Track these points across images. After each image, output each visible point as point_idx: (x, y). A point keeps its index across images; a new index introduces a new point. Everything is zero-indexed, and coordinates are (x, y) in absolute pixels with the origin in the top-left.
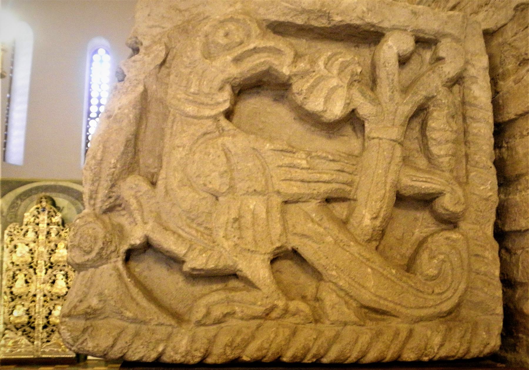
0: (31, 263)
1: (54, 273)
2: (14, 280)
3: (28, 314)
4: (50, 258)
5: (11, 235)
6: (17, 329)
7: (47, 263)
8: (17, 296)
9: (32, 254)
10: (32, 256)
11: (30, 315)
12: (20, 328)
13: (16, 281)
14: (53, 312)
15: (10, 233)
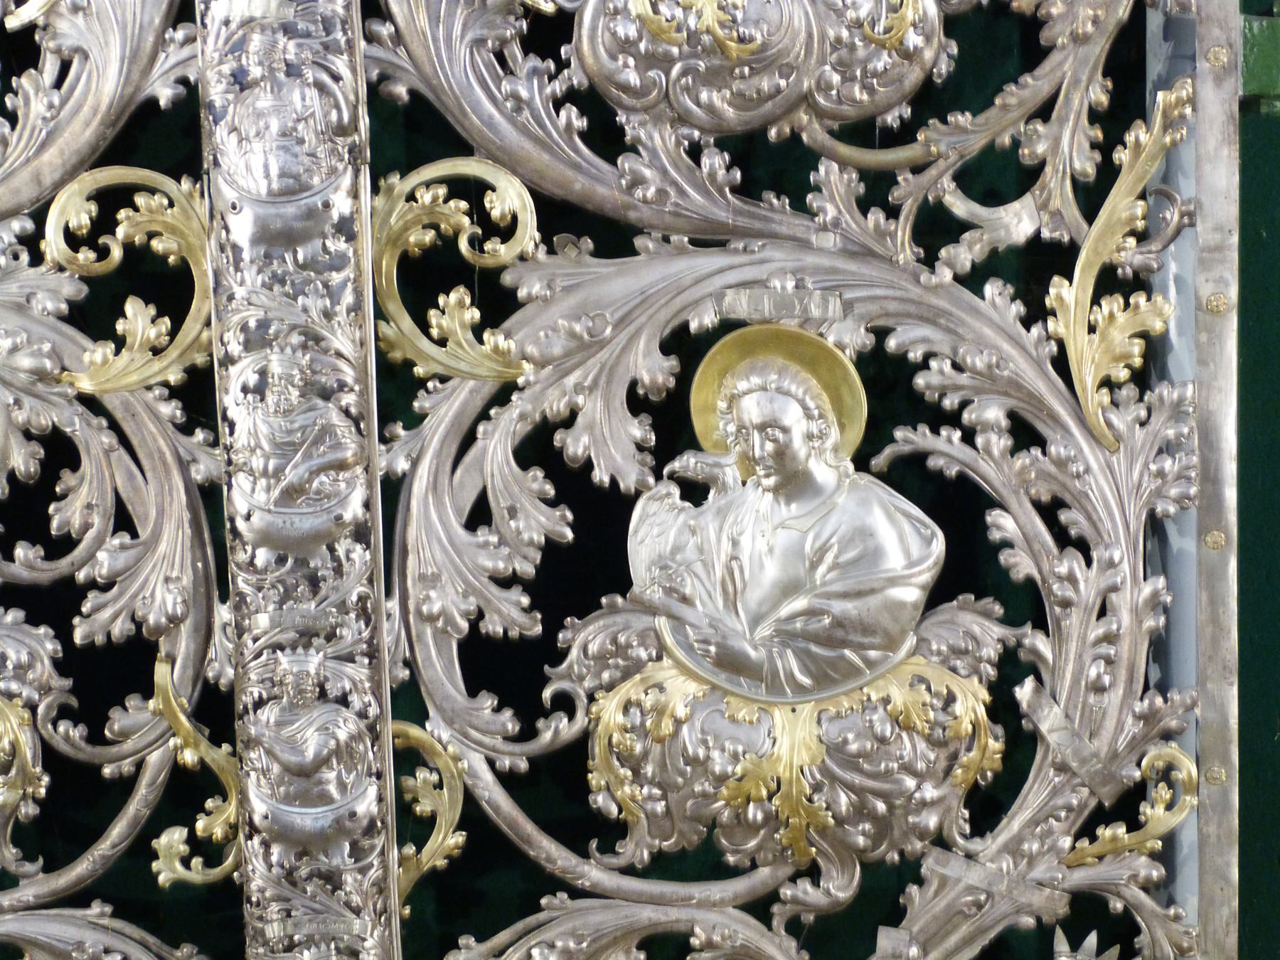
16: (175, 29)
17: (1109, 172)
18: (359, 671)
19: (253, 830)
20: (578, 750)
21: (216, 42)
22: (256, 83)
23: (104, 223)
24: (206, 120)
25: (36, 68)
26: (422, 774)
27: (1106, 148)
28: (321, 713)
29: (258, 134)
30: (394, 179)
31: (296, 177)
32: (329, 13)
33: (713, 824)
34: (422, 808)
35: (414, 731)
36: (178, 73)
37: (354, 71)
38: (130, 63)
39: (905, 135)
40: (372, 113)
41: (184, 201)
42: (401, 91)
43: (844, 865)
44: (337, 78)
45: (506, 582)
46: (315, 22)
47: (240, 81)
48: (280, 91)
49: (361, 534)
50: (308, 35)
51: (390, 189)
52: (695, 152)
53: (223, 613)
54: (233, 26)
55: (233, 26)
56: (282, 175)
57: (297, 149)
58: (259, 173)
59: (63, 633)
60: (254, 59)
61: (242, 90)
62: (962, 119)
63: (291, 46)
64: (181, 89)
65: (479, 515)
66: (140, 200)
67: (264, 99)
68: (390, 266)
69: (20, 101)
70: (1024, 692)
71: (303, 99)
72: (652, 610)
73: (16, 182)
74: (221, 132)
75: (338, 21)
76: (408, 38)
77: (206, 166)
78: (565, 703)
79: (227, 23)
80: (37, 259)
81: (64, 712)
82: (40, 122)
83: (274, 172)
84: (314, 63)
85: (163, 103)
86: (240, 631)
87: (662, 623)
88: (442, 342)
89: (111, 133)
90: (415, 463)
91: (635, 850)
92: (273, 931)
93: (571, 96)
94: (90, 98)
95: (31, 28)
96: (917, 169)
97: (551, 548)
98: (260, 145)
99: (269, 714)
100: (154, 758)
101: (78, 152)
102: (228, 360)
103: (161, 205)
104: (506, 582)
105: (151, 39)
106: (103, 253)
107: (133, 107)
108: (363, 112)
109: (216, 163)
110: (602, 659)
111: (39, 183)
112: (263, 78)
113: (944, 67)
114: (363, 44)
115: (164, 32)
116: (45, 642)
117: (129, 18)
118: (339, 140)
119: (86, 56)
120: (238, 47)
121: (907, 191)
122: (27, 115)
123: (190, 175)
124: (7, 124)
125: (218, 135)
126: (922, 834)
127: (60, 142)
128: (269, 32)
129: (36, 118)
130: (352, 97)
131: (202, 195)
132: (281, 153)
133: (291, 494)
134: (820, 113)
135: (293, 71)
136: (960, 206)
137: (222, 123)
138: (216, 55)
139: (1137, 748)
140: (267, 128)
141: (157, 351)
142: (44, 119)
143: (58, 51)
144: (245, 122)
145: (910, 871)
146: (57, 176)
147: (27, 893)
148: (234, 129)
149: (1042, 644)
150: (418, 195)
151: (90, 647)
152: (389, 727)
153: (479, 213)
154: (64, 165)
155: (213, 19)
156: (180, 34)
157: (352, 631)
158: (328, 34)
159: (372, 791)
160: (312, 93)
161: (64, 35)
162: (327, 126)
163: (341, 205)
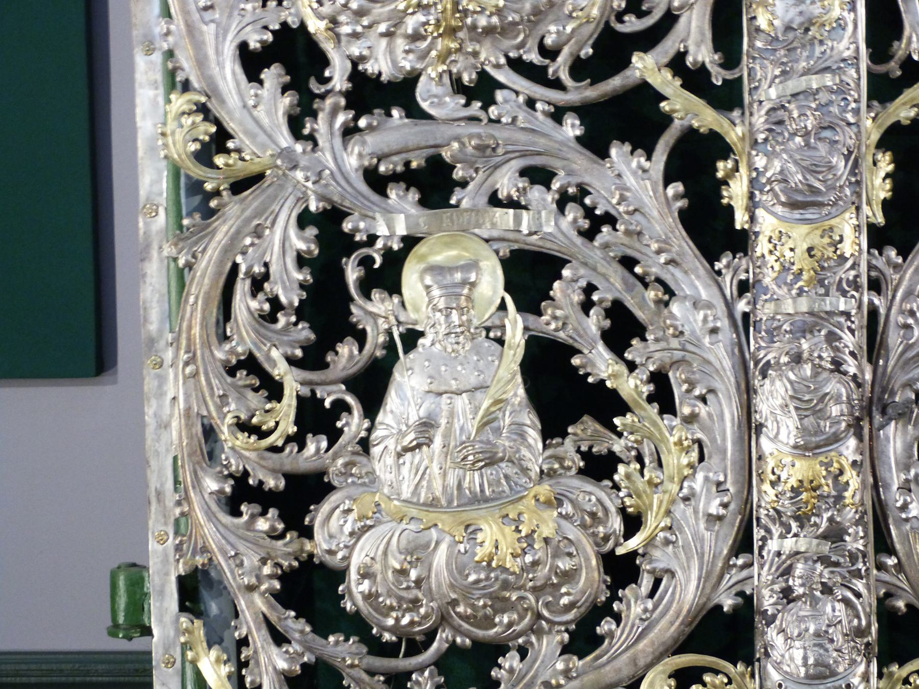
16: (737, 558)
21: (770, 569)
22: (799, 598)
24: (758, 621)
25: (636, 584)
29: (799, 635)
30: (895, 668)
31: (827, 666)
32: (854, 551)
36: (738, 588)
37: (869, 590)
38: (705, 582)
40: (878, 622)
41: (739, 678)
42: (901, 604)
44: (858, 595)
46: (843, 556)
47: (787, 595)
48: (817, 604)
50: (837, 564)
51: (891, 674)
54: (784, 557)
55: (784, 557)
56: (817, 664)
57: (828, 646)
58: (799, 661)
60: (798, 582)
61: (788, 603)
63: (826, 573)
64: (740, 600)
66: (707, 678)
67: (803, 609)
69: (623, 607)
71: (834, 610)
73: (618, 663)
74: (772, 635)
75: (860, 555)
76: (907, 568)
77: (758, 656)
79: (779, 554)
82: (637, 621)
83: (811, 661)
84: (842, 585)
85: (725, 609)
89: (688, 630)
94: (674, 605)
95: (634, 554)
98: (802, 643)
101: (663, 643)
103: (722, 682)
105: (720, 565)
107: (704, 612)
108: (874, 618)
109: (767, 655)
111: (636, 665)
112: (804, 594)
114: (875, 572)
115: (729, 560)
117: (707, 549)
118: (858, 640)
119: (672, 574)
120: (788, 572)
122: (628, 616)
123: (743, 661)
124: (614, 622)
125: (769, 635)
127: (652, 635)
128: (810, 563)
129: (635, 619)
130: (868, 610)
131: (753, 676)
132: (816, 649)
135: (827, 590)
137: (772, 626)
138: (770, 578)
140: (807, 630)
142: (641, 619)
143: (652, 572)
144: (791, 626)
146: (649, 659)
148: (782, 631)
150: (912, 680)
154: (653, 653)
155: (769, 551)
156: (740, 562)
158: (853, 565)
160: (840, 606)
161: (657, 560)
162: (850, 630)
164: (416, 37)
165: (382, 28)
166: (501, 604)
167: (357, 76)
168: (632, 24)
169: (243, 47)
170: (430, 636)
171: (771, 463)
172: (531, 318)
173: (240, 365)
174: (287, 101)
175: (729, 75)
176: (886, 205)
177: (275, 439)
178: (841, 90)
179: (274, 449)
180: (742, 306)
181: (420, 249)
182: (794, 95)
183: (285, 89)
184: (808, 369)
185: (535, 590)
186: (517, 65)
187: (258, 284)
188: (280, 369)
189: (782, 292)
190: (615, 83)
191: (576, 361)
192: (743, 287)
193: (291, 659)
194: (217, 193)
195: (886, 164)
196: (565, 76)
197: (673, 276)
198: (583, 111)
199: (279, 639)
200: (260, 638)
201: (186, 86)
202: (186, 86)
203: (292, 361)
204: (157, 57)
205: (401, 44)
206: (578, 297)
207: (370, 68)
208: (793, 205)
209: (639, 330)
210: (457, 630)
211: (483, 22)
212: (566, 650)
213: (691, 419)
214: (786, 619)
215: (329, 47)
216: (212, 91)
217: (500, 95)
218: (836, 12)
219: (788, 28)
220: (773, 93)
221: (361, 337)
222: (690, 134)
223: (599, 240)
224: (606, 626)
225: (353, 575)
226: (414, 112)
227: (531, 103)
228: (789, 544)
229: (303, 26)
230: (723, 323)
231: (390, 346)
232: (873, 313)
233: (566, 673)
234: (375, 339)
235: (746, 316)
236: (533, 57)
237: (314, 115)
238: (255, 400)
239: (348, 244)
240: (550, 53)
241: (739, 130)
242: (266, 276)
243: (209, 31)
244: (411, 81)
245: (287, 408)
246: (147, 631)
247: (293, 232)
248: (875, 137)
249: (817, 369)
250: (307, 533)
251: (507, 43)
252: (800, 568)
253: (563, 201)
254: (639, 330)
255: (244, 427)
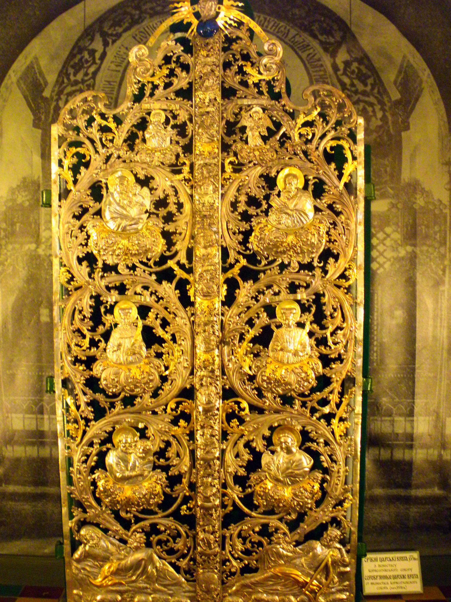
0: (163, 259)
1: (267, 299)
2: (101, 329)
3: (166, 469)
4: (247, 234)
5: (79, 144)
6: (126, 524)
7: (232, 255)
8: (115, 396)
9: (169, 218)
10: (170, 228)
11: (173, 472)
12: (138, 520)
13: (107, 336)
14: (266, 459)
15: (72, 136)
17: (341, 402)
18: (216, 481)
19: (198, 506)
20: (252, 494)
23: (177, 407)
24: (195, 391)
26: (226, 498)
27: (340, 398)
28: (210, 488)
33: (274, 506)
34: (226, 503)
35: (225, 490)
39: (309, 395)
42: (227, 387)
43: (295, 513)
45: (241, 467)
47: (202, 385)
49: (218, 459)
52: (275, 398)
53: (194, 471)
59: (167, 474)
62: (318, 393)
65: (237, 456)
68: (224, 415)
70: (325, 485)
72: (265, 472)
74: (198, 394)
78: (250, 486)
80: (166, 412)
81: (167, 486)
86: (197, 474)
87: (267, 474)
88: (232, 428)
90: (227, 447)
91: (261, 510)
92: (201, 523)
93: (255, 388)
95: (166, 376)
96: (310, 401)
97: (249, 461)
99: (202, 488)
100: (181, 494)
102: (197, 430)
104: (241, 467)
106: (177, 412)
110: (256, 480)
113: (315, 385)
116: (164, 475)
120: (202, 380)
121: (309, 404)
126: (308, 508)
133: (208, 452)
134: (295, 392)
135: (211, 384)
136: (317, 407)
139: (343, 494)
141: (185, 428)
145: (305, 514)
147: (160, 515)
149: (328, 477)
151: (172, 476)
152: (221, 490)
153: (239, 407)
157: (216, 474)
159: (218, 501)
160: (214, 388)
163: (217, 406)
164: (118, 255)
165: (110, 253)
166: (136, 387)
167: (105, 264)
168: (168, 254)
169: (78, 257)
170: (120, 394)
171: (198, 355)
172: (144, 321)
173: (76, 331)
174: (88, 269)
175: (191, 266)
176: (225, 296)
177: (83, 348)
178: (216, 270)
179: (84, 350)
180: (192, 319)
181: (118, 304)
182: (205, 271)
183: (87, 267)
184: (207, 333)
185: (144, 384)
186: (141, 262)
187: (80, 312)
188: (86, 332)
189: (201, 316)
190: (164, 267)
191: (154, 331)
192: (193, 314)
193: (88, 399)
194: (71, 291)
195: (225, 287)
196: (152, 265)
197: (177, 312)
198: (156, 273)
199: (85, 394)
200: (81, 394)
201: (65, 266)
202: (65, 266)
203: (88, 330)
204: (58, 259)
205: (114, 257)
206: (154, 316)
207: (108, 262)
208: (204, 296)
209: (168, 324)
210: (126, 392)
211: (134, 252)
212: (151, 397)
213: (180, 345)
214: (202, 390)
215: (98, 257)
216: (71, 267)
217: (137, 269)
218: (214, 252)
219: (204, 255)
220: (200, 270)
221: (104, 325)
222: (181, 280)
223: (160, 303)
224: (160, 392)
225: (102, 380)
226: (117, 273)
227: (144, 271)
228: (202, 373)
229: (92, 252)
230: (188, 323)
231: (111, 327)
232: (222, 321)
233: (151, 402)
234: (108, 325)
235: (193, 321)
236: (145, 260)
237: (94, 273)
238: (79, 339)
239: (102, 303)
240: (149, 260)
241: (192, 278)
242: (82, 310)
243: (70, 253)
244: (117, 265)
245: (87, 341)
246: (54, 392)
247: (89, 300)
248: (223, 281)
249: (209, 333)
250: (91, 370)
251: (139, 257)
252: (205, 379)
253: (152, 294)
254: (168, 324)
255: (77, 345)
